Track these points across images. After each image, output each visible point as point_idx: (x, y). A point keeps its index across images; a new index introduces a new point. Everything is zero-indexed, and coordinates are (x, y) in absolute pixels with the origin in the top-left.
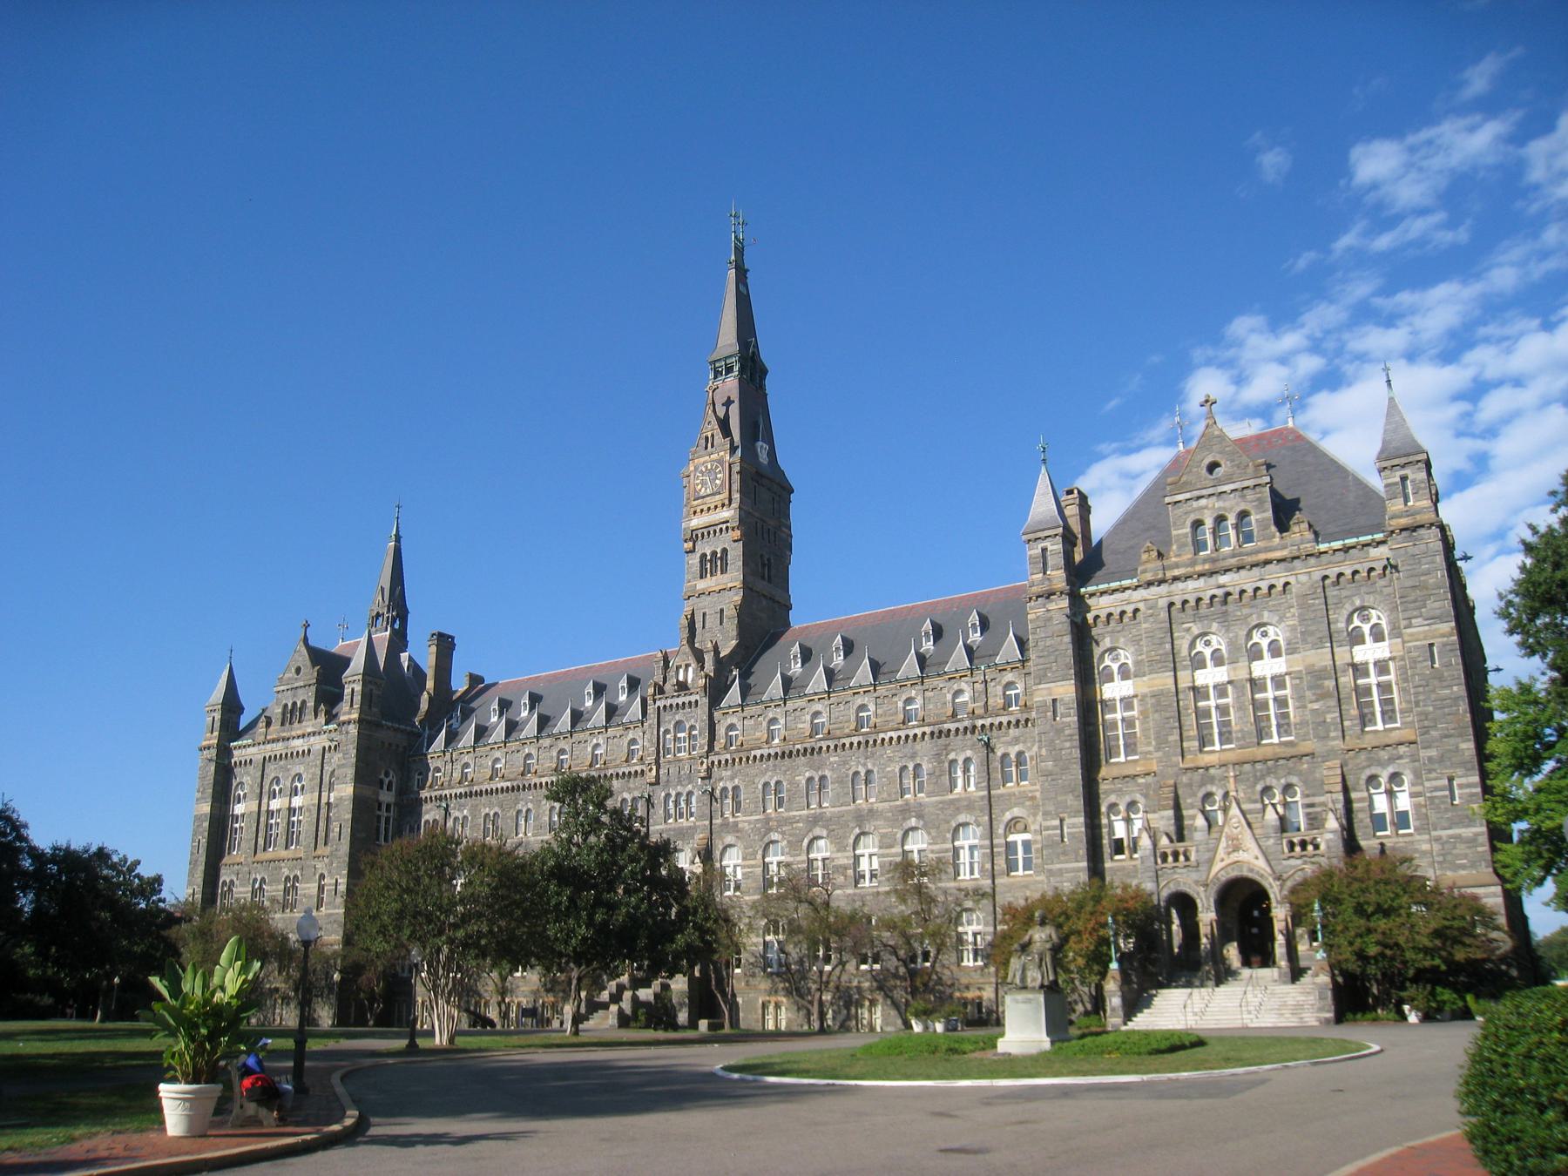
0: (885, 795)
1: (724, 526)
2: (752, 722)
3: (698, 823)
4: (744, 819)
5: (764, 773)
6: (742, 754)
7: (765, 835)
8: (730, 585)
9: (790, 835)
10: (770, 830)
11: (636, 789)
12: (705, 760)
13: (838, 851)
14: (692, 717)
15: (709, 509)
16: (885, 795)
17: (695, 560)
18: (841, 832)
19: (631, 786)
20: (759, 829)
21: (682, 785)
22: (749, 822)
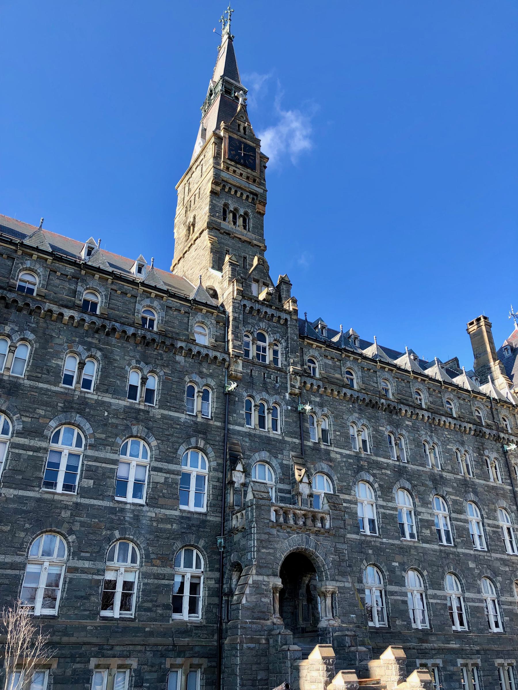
0: (449, 468)
1: (251, 196)
2: (330, 363)
3: (287, 439)
4: (336, 449)
5: (351, 412)
6: (334, 387)
7: (358, 473)
8: (255, 242)
9: (381, 479)
10: (360, 469)
11: (211, 376)
12: (298, 378)
13: (422, 506)
14: (278, 332)
15: (241, 175)
16: (449, 468)
17: (220, 204)
18: (422, 489)
19: (205, 370)
20: (350, 463)
21: (268, 393)
22: (341, 454)
